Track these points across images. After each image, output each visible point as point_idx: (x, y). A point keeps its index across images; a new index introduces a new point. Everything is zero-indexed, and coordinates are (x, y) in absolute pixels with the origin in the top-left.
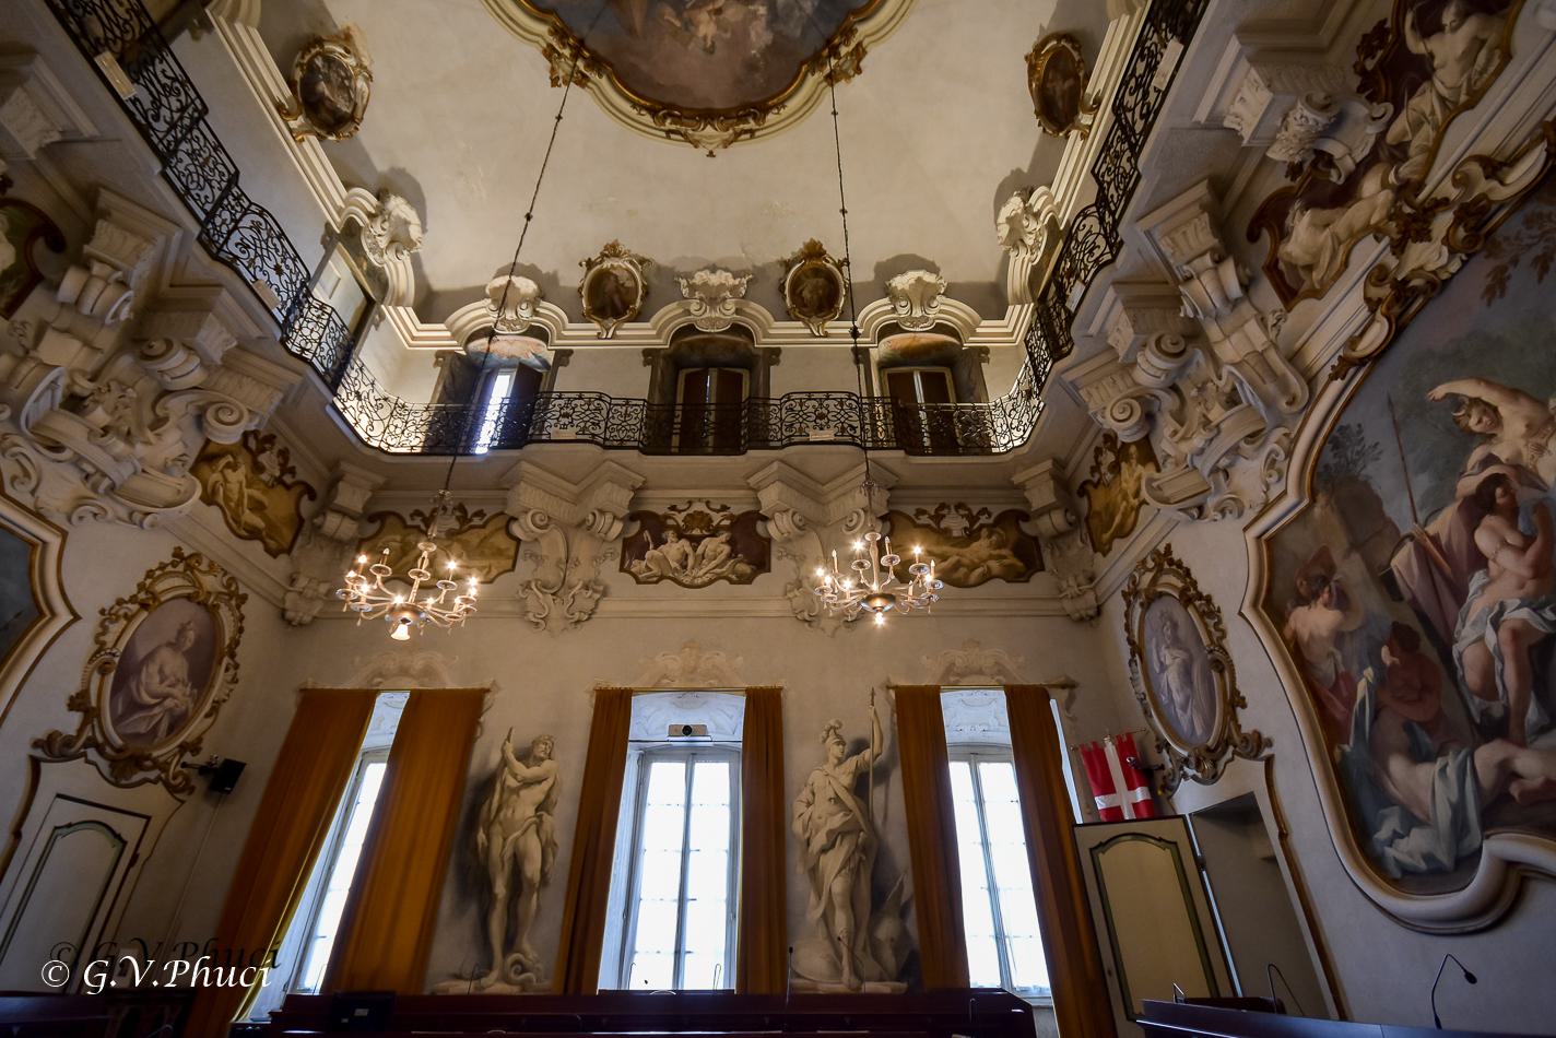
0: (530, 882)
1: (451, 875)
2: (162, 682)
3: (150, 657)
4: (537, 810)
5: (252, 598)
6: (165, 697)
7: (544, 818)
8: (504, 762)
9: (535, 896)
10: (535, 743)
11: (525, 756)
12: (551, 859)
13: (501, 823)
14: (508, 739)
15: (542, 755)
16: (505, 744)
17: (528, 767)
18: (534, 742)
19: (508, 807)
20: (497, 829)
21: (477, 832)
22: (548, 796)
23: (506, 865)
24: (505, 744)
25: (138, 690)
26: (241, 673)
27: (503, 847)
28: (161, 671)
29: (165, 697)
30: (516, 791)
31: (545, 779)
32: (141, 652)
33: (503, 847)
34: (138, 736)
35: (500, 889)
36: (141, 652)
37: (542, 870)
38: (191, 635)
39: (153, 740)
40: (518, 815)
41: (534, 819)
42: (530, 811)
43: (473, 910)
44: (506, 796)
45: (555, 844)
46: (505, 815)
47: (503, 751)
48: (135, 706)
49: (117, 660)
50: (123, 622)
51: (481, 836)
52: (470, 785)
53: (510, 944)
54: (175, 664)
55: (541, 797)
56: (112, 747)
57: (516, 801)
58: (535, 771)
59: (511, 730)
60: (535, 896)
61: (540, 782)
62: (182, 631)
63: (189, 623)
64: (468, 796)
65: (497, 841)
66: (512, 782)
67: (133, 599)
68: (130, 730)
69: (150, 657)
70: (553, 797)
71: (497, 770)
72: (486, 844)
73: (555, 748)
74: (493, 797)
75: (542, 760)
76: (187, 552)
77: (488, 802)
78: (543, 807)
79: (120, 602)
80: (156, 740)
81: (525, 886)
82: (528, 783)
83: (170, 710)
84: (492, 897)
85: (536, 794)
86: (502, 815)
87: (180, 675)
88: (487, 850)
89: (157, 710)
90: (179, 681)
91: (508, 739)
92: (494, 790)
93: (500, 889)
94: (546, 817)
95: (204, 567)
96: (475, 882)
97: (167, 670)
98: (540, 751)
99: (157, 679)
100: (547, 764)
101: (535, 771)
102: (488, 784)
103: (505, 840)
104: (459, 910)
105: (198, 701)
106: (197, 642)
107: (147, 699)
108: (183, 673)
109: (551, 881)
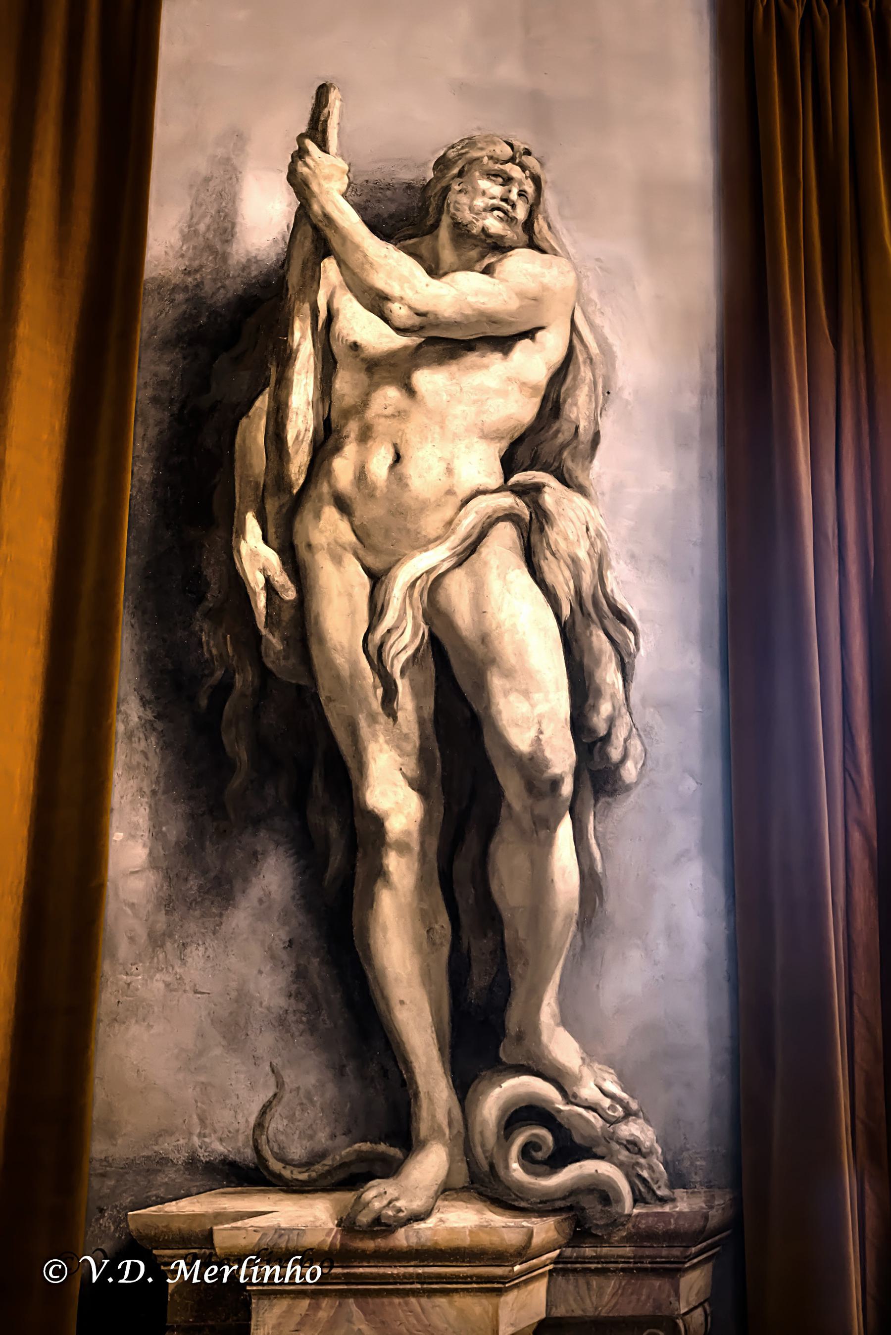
0: (531, 768)
1: (129, 713)
4: (509, 463)
7: (549, 499)
8: (313, 236)
9: (565, 830)
10: (454, 167)
11: (412, 216)
12: (609, 676)
13: (343, 505)
14: (317, 130)
15: (494, 224)
16: (301, 154)
17: (434, 271)
18: (442, 164)
19: (366, 435)
20: (327, 528)
21: (236, 531)
22: (552, 404)
23: (403, 686)
24: (301, 154)
27: (376, 611)
30: (395, 369)
31: (530, 334)
33: (376, 611)
35: (392, 793)
37: (579, 724)
40: (425, 473)
41: (507, 500)
42: (480, 466)
43: (274, 878)
44: (345, 384)
45: (622, 617)
46: (361, 476)
47: (299, 184)
51: (256, 555)
52: (153, 317)
53: (481, 1034)
55: (523, 410)
57: (400, 415)
58: (461, 293)
59: (322, 92)
60: (565, 830)
61: (503, 343)
64: (150, 373)
65: (340, 592)
66: (360, 326)
70: (579, 408)
71: (285, 262)
72: (291, 594)
73: (549, 197)
74: (283, 384)
75: (498, 247)
77: (263, 402)
78: (539, 449)
81: (512, 786)
82: (445, 342)
84: (365, 833)
85: (499, 390)
86: (343, 468)
88: (300, 620)
91: (317, 130)
92: (285, 358)
93: (392, 793)
94: (554, 495)
96: (262, 753)
98: (480, 203)
100: (520, 265)
101: (461, 293)
102: (245, 325)
103: (377, 579)
104: (202, 877)
109: (630, 772)
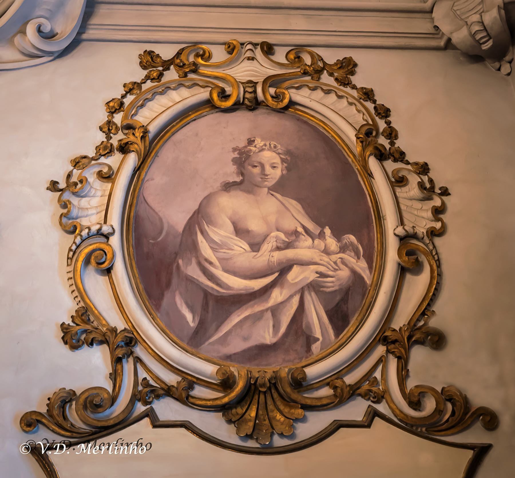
2: (255, 247)
3: (199, 218)
5: (356, 56)
6: (284, 269)
25: (211, 277)
26: (440, 176)
28: (240, 231)
29: (284, 269)
32: (175, 216)
34: (262, 350)
36: (175, 216)
38: (268, 157)
39: (309, 350)
48: (218, 305)
49: (115, 241)
50: (98, 188)
54: (270, 212)
56: (207, 385)
62: (243, 159)
63: (251, 142)
67: (105, 150)
68: (237, 345)
69: (199, 218)
76: (166, 52)
79: (78, 162)
80: (316, 348)
83: (314, 287)
87: (290, 224)
89: (277, 296)
90: (296, 233)
95: (219, 54)
97: (255, 226)
99: (240, 246)
105: (374, 256)
106: (292, 161)
107: (237, 284)
108: (294, 215)
